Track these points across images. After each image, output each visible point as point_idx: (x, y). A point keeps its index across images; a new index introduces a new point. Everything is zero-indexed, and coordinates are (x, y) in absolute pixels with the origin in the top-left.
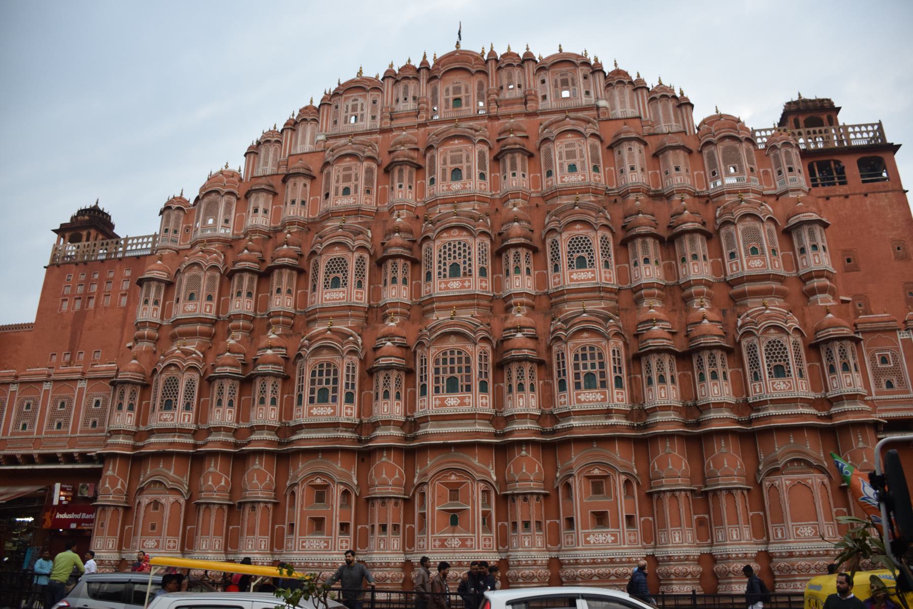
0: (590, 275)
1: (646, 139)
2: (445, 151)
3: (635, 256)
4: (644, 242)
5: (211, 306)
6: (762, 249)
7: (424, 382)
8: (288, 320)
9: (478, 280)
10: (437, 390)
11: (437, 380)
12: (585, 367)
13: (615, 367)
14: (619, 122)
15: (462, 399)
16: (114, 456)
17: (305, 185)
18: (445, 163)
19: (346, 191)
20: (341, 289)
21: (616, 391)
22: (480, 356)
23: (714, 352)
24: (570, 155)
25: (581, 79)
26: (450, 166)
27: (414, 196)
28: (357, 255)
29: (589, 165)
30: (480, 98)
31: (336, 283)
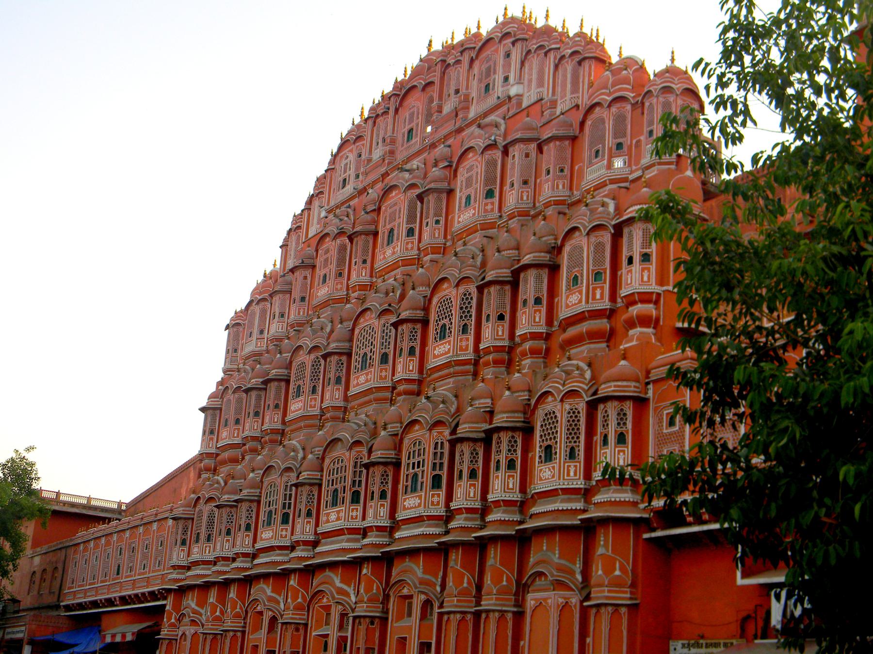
0: (447, 347)
2: (386, 210)
5: (238, 429)
6: (582, 277)
8: (274, 437)
15: (338, 512)
16: (169, 591)
17: (305, 278)
20: (301, 398)
22: (356, 463)
23: (501, 434)
24: (469, 182)
26: (389, 227)
28: (313, 356)
29: (481, 194)
30: (428, 122)
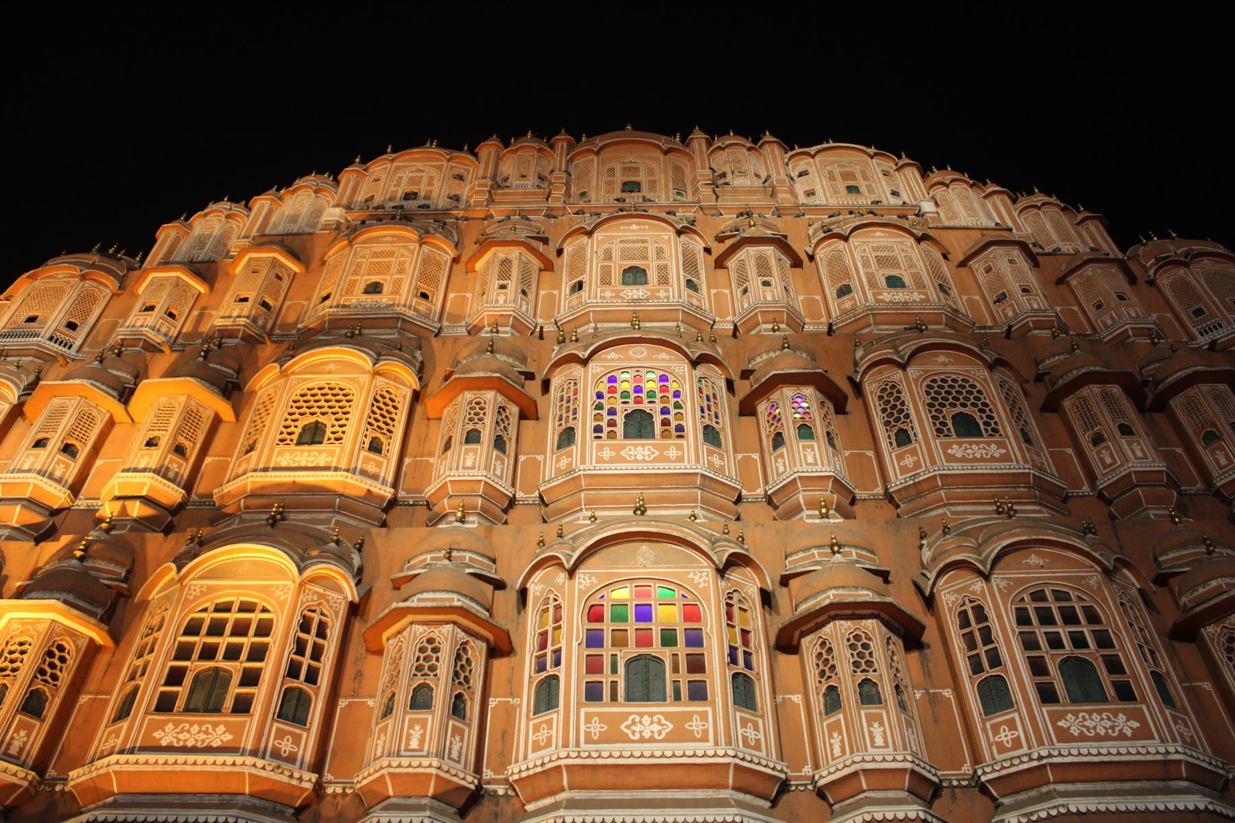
0: (995, 451)
1: (1039, 258)
3: (1090, 421)
4: (1106, 396)
7: (551, 670)
9: (705, 448)
10: (593, 693)
11: (594, 666)
12: (1055, 642)
13: (1141, 647)
14: (971, 232)
18: (608, 256)
19: (375, 288)
21: (1167, 712)
25: (881, 175)
27: (531, 312)
31: (313, 435)
